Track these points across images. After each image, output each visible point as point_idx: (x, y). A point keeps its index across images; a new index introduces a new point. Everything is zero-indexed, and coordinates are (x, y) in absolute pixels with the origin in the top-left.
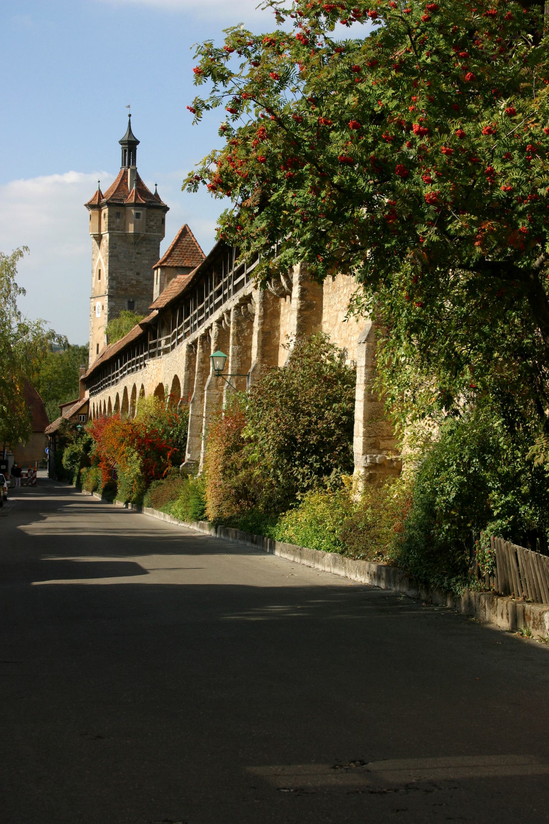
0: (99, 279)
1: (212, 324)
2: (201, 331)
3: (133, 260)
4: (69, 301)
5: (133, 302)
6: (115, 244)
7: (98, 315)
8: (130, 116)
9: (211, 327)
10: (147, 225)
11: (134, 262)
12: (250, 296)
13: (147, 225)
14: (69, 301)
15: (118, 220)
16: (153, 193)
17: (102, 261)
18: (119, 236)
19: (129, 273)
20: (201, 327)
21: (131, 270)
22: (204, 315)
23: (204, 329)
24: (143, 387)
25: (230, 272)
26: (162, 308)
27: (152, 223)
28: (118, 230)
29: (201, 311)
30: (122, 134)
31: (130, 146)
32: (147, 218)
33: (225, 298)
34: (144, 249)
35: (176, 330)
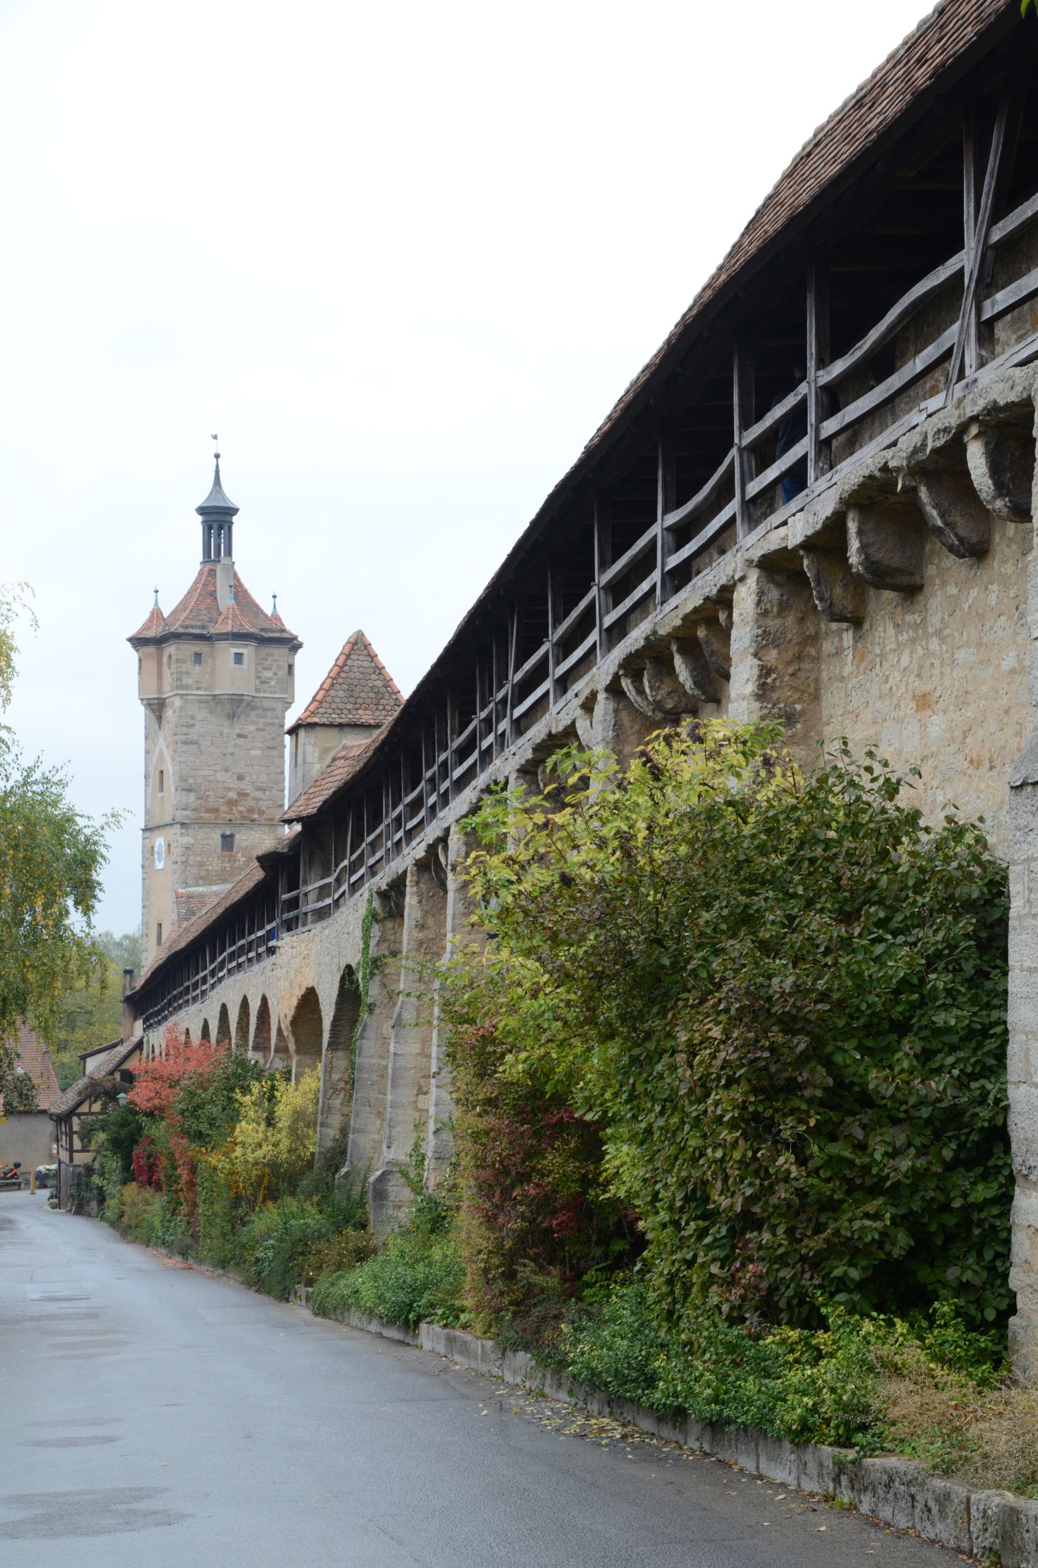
0: (162, 790)
1: (447, 830)
2: (417, 850)
3: (230, 750)
4: (89, 746)
5: (232, 836)
6: (193, 718)
7: (160, 865)
8: (217, 456)
9: (443, 840)
10: (258, 678)
11: (232, 754)
12: (570, 732)
13: (258, 678)
14: (89, 746)
15: (198, 669)
16: (269, 612)
17: (165, 751)
20: (414, 843)
21: (227, 770)
22: (422, 813)
23: (423, 845)
24: (264, 1000)
25: (501, 686)
26: (310, 817)
27: (268, 674)
28: (198, 689)
29: (416, 806)
30: (201, 496)
31: (218, 519)
32: (257, 664)
33: (487, 756)
34: (252, 728)
35: (346, 862)
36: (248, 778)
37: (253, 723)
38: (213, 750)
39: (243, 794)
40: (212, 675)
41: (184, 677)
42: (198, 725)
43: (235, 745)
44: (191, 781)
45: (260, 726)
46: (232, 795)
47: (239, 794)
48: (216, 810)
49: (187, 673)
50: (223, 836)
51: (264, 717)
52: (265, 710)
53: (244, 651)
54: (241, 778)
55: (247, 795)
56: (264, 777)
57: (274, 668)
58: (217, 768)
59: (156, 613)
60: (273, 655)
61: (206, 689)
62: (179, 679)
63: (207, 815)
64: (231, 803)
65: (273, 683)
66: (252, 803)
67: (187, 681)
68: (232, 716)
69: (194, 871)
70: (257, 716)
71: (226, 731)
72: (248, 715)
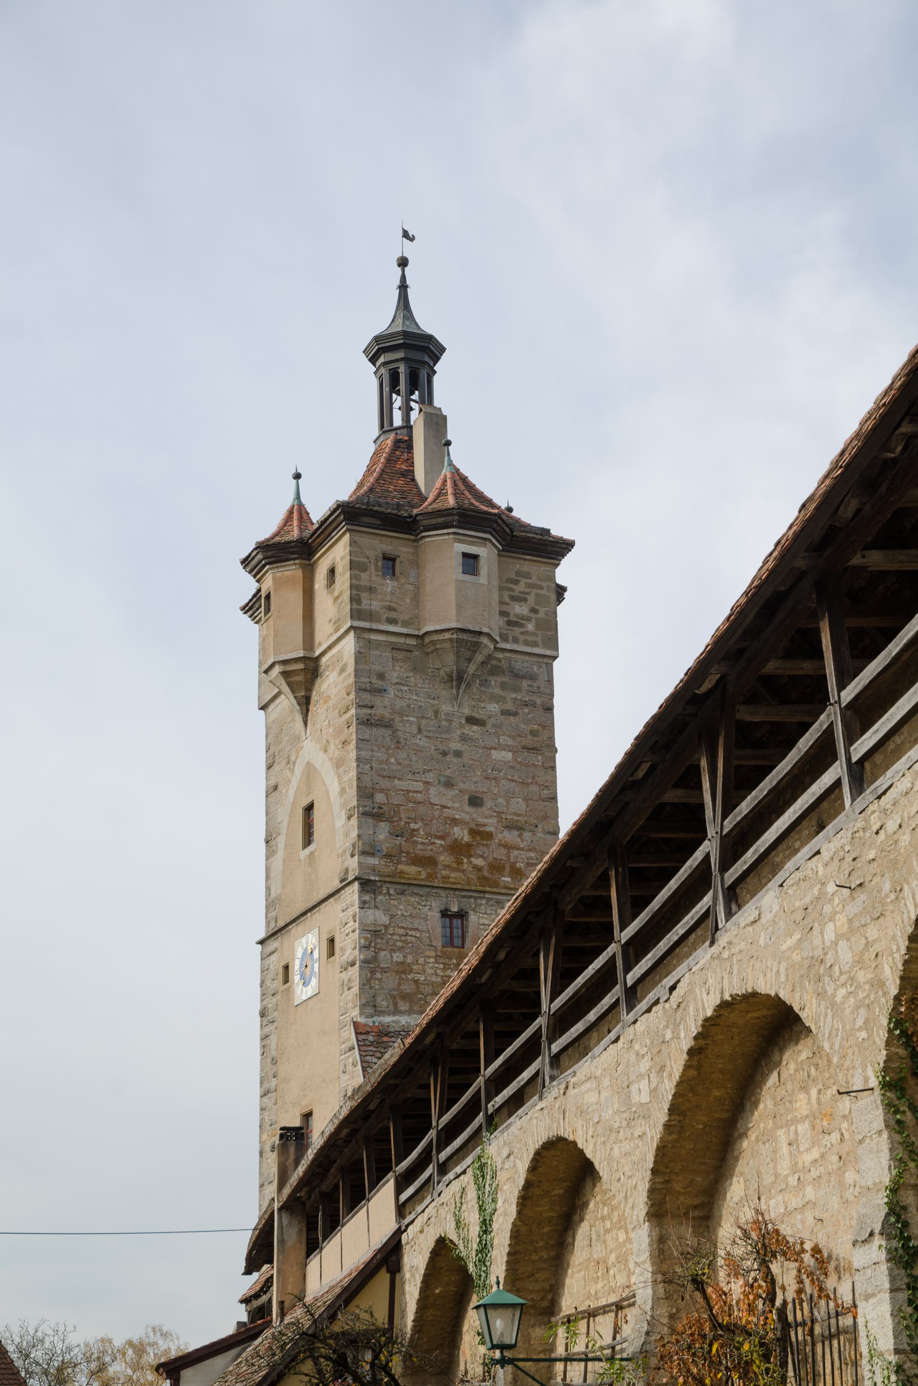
3: (455, 745)
5: (462, 915)
6: (381, 676)
11: (458, 754)
18: (395, 648)
19: (436, 795)
27: (520, 609)
28: (391, 621)
31: (407, 358)
34: (494, 708)
36: (489, 804)
37: (495, 698)
38: (422, 742)
39: (480, 834)
40: (417, 598)
41: (364, 596)
42: (392, 691)
43: (464, 738)
44: (380, 798)
45: (509, 706)
46: (461, 834)
47: (473, 832)
48: (429, 862)
49: (371, 590)
50: (445, 913)
51: (517, 689)
52: (517, 676)
53: (483, 551)
54: (475, 801)
55: (489, 836)
56: (518, 805)
57: (531, 599)
58: (430, 777)
59: (298, 511)
60: (528, 576)
61: (405, 624)
62: (355, 599)
63: (412, 870)
64: (459, 850)
65: (530, 627)
66: (500, 854)
67: (373, 604)
68: (458, 679)
69: (390, 981)
70: (503, 686)
71: (446, 708)
72: (485, 683)
